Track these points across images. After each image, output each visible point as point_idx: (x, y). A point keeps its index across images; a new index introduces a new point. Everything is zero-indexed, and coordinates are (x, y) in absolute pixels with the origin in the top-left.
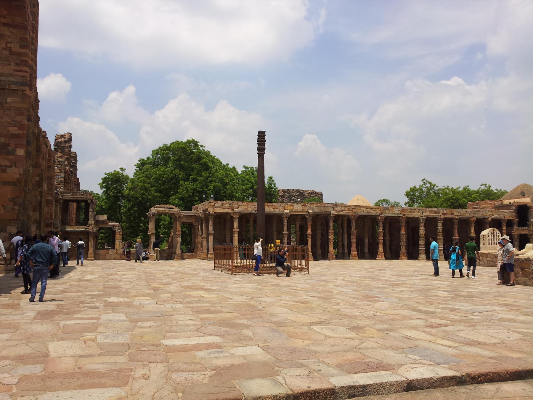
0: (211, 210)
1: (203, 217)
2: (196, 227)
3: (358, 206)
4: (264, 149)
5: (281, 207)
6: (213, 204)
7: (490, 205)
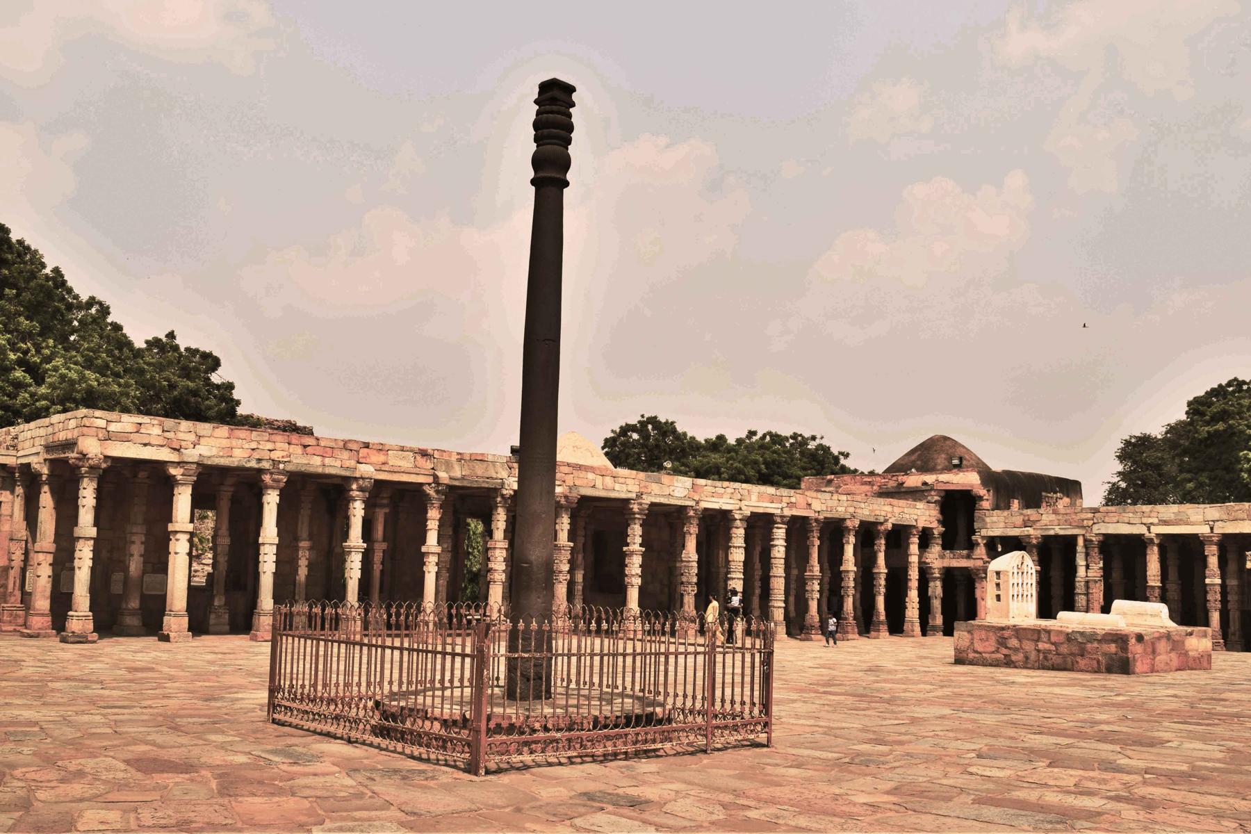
0: (92, 447)
1: (45, 471)
2: (6, 509)
3: (579, 467)
4: (566, 164)
5: (346, 455)
6: (102, 423)
7: (867, 488)
